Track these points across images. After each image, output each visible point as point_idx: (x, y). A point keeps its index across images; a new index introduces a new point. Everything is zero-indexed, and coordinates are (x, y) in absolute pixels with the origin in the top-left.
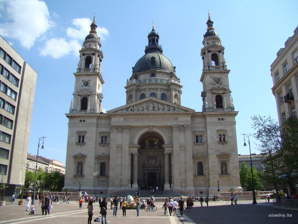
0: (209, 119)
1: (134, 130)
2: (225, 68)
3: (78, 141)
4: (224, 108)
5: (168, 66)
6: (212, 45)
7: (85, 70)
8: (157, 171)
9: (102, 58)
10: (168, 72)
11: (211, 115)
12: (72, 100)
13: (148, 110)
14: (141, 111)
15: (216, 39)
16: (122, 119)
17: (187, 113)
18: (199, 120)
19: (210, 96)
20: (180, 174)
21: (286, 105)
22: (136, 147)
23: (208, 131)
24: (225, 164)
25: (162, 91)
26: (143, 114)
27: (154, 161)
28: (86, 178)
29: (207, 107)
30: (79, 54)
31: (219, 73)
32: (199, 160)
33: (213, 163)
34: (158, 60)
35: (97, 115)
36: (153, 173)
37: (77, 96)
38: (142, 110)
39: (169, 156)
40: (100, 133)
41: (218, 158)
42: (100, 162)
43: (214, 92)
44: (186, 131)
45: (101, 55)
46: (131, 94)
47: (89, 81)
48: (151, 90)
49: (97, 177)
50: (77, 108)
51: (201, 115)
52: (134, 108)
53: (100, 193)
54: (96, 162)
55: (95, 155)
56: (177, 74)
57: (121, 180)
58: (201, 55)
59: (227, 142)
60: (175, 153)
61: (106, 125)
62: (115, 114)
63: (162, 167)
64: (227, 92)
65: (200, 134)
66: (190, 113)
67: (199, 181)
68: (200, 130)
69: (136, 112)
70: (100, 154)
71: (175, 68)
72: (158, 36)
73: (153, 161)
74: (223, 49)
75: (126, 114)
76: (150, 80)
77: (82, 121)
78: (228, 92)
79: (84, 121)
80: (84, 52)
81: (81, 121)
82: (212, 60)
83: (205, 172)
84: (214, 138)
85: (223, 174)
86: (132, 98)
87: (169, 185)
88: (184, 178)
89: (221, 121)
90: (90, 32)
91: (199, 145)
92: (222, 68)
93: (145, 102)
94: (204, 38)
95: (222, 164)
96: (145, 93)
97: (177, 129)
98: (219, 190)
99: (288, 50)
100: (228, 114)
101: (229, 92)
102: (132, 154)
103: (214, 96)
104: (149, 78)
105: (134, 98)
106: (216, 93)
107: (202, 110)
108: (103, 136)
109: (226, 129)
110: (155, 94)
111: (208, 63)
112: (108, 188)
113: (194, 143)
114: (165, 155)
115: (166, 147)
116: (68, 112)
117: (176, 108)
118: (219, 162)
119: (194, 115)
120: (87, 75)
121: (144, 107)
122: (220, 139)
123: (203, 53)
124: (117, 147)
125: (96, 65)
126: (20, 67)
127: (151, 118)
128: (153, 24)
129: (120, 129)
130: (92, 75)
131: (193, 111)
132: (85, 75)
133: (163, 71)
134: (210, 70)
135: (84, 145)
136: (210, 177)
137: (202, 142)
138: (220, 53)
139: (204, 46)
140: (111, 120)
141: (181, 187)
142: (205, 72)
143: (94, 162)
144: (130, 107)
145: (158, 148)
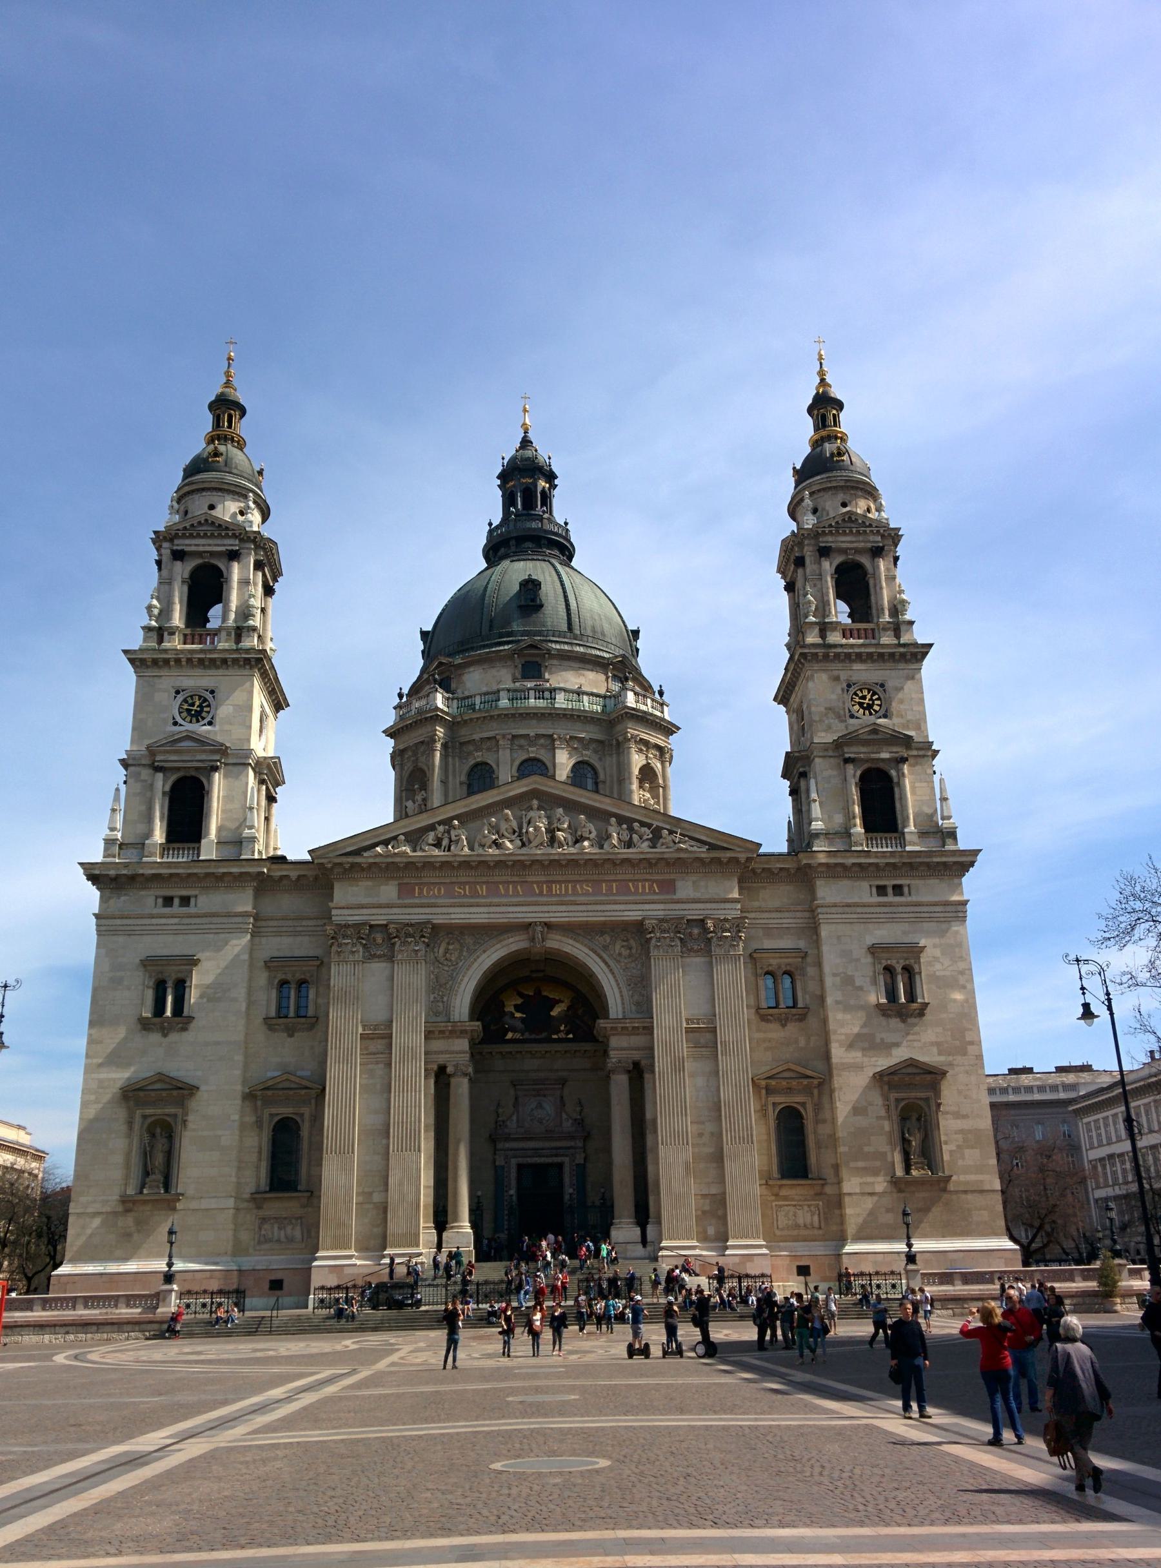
0: (828, 892)
1: (448, 944)
4: (903, 834)
5: (606, 626)
6: (839, 520)
7: (189, 637)
8: (566, 1160)
9: (275, 580)
10: (606, 655)
11: (839, 869)
12: (117, 790)
13: (523, 845)
14: (490, 847)
15: (857, 488)
16: (389, 891)
17: (718, 861)
18: (775, 896)
19: (835, 773)
22: (463, 1032)
23: (825, 948)
24: (919, 1119)
26: (500, 864)
28: (194, 1205)
29: (817, 825)
31: (873, 661)
32: (783, 1100)
34: (556, 597)
35: (259, 870)
37: (145, 773)
38: (495, 842)
39: (630, 1079)
40: (271, 964)
41: (881, 1088)
42: (271, 1115)
43: (850, 752)
44: (716, 950)
46: (420, 764)
47: (212, 692)
48: (521, 747)
49: (254, 1199)
50: (149, 834)
51: (787, 869)
52: (453, 833)
53: (267, 1286)
54: (250, 1119)
55: (244, 1082)
57: (385, 1210)
58: (779, 571)
60: (661, 1062)
61: (304, 923)
62: (353, 866)
64: (915, 753)
65: (789, 964)
66: (736, 860)
67: (792, 1209)
68: (786, 943)
70: (270, 1074)
71: (636, 634)
72: (551, 477)
74: (895, 537)
77: (176, 901)
78: (924, 756)
79: (185, 901)
81: (168, 901)
84: (858, 984)
85: (914, 1173)
86: (424, 786)
87: (638, 1230)
89: (891, 898)
90: (211, 440)
92: (887, 639)
93: (509, 803)
95: (904, 1119)
97: (672, 939)
98: (911, 1258)
100: (928, 865)
101: (930, 753)
103: (853, 774)
104: (510, 685)
106: (861, 760)
107: (786, 844)
108: (289, 977)
110: (544, 764)
112: (316, 1259)
113: (758, 1009)
115: (615, 1028)
116: (98, 857)
118: (888, 1110)
119: (753, 870)
120: (201, 661)
121: (504, 826)
125: (245, 613)
127: (537, 883)
128: (525, 411)
130: (224, 661)
131: (748, 845)
132: (189, 660)
133: (582, 649)
135: (184, 1029)
136: (847, 1187)
137: (795, 1006)
138: (876, 560)
139: (793, 526)
140: (332, 901)
141: (698, 1241)
142: (803, 655)
143: (236, 1117)
144: (432, 828)
145: (571, 1036)
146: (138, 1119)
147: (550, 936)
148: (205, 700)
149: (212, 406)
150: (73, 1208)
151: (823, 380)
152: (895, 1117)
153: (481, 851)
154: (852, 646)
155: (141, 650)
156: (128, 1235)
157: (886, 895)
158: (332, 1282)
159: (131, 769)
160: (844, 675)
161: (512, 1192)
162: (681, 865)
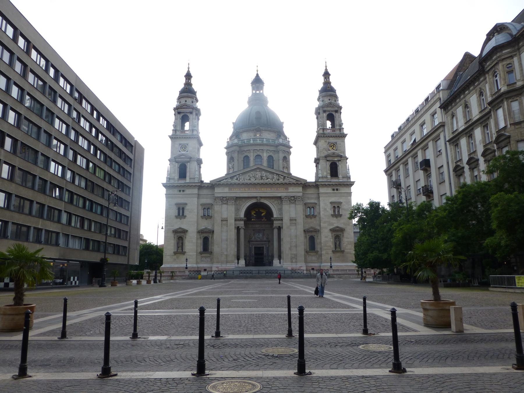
0: (322, 190)
2: (342, 131)
3: (177, 215)
8: (265, 246)
10: (276, 130)
15: (332, 96)
16: (226, 190)
20: (290, 249)
21: (395, 190)
23: (321, 202)
25: (268, 152)
27: (261, 235)
28: (188, 254)
30: (174, 112)
32: (310, 234)
33: (326, 237)
36: (260, 247)
37: (174, 163)
38: (249, 179)
43: (328, 159)
44: (297, 203)
45: (198, 112)
47: (187, 144)
51: (313, 185)
52: (240, 177)
54: (199, 237)
55: (197, 229)
56: (287, 131)
58: (315, 114)
59: (342, 215)
62: (219, 184)
63: (270, 241)
64: (342, 159)
68: (312, 201)
69: (241, 181)
73: (260, 235)
74: (341, 108)
75: (232, 184)
76: (254, 140)
77: (182, 191)
79: (183, 191)
80: (180, 110)
81: (180, 191)
82: (327, 120)
83: (318, 247)
86: (233, 161)
88: (295, 253)
89: (335, 191)
90: (185, 84)
91: (311, 218)
94: (320, 94)
96: (248, 155)
98: (331, 267)
99: (396, 141)
100: (344, 184)
102: (238, 227)
103: (329, 164)
104: (253, 137)
105: (236, 161)
108: (206, 207)
109: (341, 201)
110: (261, 156)
111: (322, 125)
114: (274, 228)
116: (165, 182)
117: (286, 177)
119: (306, 185)
120: (185, 137)
121: (251, 175)
122: (334, 211)
123: (318, 112)
124: (222, 221)
126: (132, 146)
128: (257, 66)
129: (224, 200)
130: (190, 137)
132: (182, 137)
134: (324, 134)
135: (185, 218)
136: (323, 253)
142: (319, 136)
143: (196, 236)
144: (236, 176)
146: (176, 237)
147: (262, 199)
148: (186, 146)
149: (185, 76)
150: (164, 254)
151: (326, 70)
152: (334, 239)
153: (246, 181)
154: (330, 134)
155: (172, 135)
156: (175, 260)
157: (334, 191)
158: (217, 269)
159: (171, 162)
160: (328, 141)
161: (253, 252)
162: (290, 184)
